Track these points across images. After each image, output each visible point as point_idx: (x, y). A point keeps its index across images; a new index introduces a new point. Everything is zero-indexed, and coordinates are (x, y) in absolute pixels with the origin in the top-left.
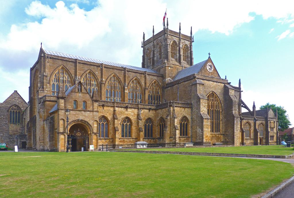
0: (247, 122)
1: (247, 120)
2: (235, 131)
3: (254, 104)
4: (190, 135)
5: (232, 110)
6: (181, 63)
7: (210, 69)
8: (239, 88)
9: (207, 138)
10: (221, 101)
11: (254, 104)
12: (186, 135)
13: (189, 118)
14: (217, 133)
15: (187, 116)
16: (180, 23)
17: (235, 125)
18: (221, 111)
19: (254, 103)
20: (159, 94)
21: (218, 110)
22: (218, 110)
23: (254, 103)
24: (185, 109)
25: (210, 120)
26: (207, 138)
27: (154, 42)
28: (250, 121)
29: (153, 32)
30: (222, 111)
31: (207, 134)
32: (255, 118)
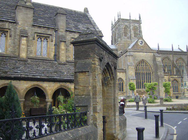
2: (160, 88)
4: (124, 91)
7: (141, 44)
10: (151, 66)
12: (123, 91)
13: (124, 79)
17: (160, 83)
22: (149, 72)
25: (135, 80)
29: (115, 21)
30: (152, 73)
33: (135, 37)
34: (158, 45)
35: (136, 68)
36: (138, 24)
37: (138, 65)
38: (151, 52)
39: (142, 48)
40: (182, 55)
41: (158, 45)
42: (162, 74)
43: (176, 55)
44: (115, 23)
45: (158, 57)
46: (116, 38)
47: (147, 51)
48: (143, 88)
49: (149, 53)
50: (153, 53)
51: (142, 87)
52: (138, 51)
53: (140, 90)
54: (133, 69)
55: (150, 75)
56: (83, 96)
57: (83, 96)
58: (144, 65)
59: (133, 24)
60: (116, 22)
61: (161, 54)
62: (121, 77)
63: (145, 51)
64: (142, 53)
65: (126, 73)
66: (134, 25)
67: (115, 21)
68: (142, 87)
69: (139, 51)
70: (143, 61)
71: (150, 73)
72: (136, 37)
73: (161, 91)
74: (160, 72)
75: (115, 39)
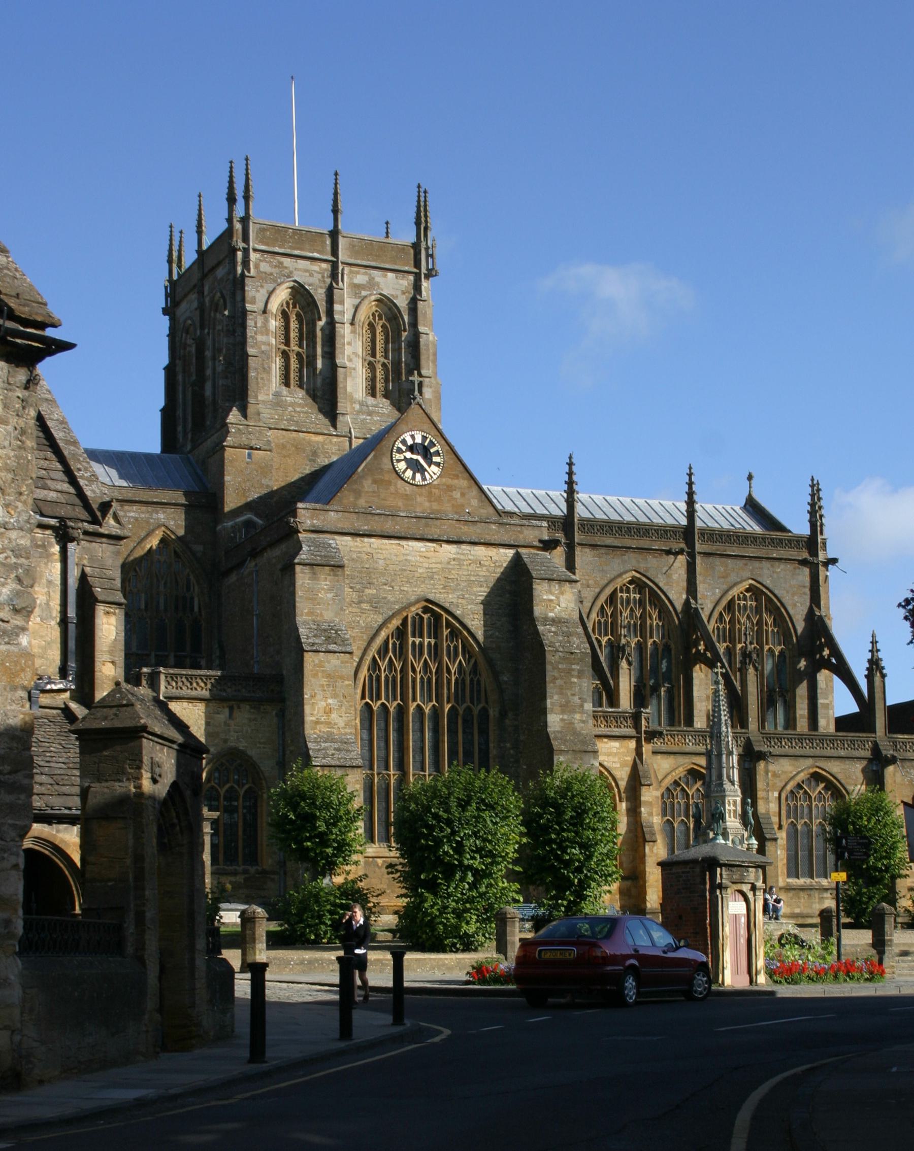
0: (816, 777)
1: (810, 762)
3: (874, 650)
5: (544, 712)
6: (340, 418)
8: (812, 543)
11: (874, 650)
12: (253, 857)
15: (249, 752)
16: (336, 174)
18: (493, 713)
19: (874, 642)
20: (196, 609)
22: (476, 710)
23: (874, 642)
24: (236, 713)
27: (201, 293)
28: (835, 768)
29: (200, 232)
30: (503, 715)
32: (876, 749)
34: (570, 473)
35: (364, 672)
37: (383, 650)
38: (496, 539)
40: (766, 564)
41: (570, 473)
42: (578, 726)
43: (717, 561)
44: (200, 252)
45: (556, 587)
46: (208, 392)
47: (465, 528)
49: (480, 551)
50: (511, 553)
52: (389, 526)
54: (342, 678)
55: (484, 732)
56: (110, 884)
57: (110, 884)
59: (361, 278)
60: (207, 242)
61: (594, 546)
62: (242, 745)
65: (281, 714)
67: (200, 232)
69: (397, 529)
71: (484, 712)
74: (566, 708)
75: (198, 398)
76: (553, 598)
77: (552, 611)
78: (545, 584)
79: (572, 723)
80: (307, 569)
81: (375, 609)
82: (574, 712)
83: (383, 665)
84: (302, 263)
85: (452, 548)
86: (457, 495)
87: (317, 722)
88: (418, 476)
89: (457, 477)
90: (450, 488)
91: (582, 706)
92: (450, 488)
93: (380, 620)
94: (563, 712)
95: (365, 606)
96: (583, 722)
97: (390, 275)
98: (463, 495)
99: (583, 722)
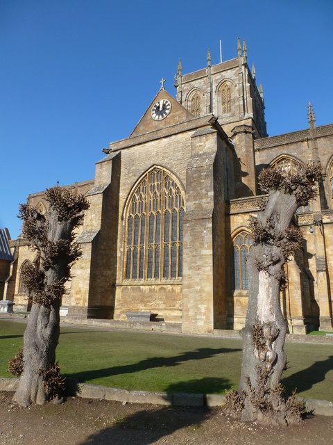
9: (79, 296)
14: (169, 281)
21: (177, 210)
26: (79, 296)
31: (81, 285)
33: (224, 111)
36: (234, 71)
38: (187, 128)
39: (162, 126)
48: (149, 276)
49: (180, 136)
51: (145, 271)
52: (142, 139)
53: (137, 281)
58: (159, 187)
59: (218, 76)
63: (165, 132)
64: (153, 143)
66: (222, 76)
68: (145, 271)
70: (154, 173)
72: (230, 110)
73: (189, 287)
74: (198, 196)
76: (201, 144)
77: (201, 151)
78: (198, 139)
79: (200, 205)
80: (99, 165)
81: (134, 175)
82: (202, 198)
83: (137, 198)
84: (197, 81)
85: (167, 139)
86: (177, 118)
87: (88, 225)
88: (161, 117)
89: (177, 111)
90: (174, 116)
91: (207, 194)
92: (174, 116)
93: (136, 179)
94: (195, 200)
95: (131, 175)
96: (208, 203)
97: (229, 71)
98: (179, 117)
99: (208, 203)
